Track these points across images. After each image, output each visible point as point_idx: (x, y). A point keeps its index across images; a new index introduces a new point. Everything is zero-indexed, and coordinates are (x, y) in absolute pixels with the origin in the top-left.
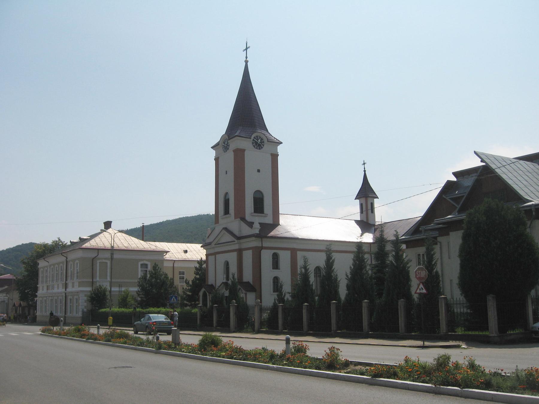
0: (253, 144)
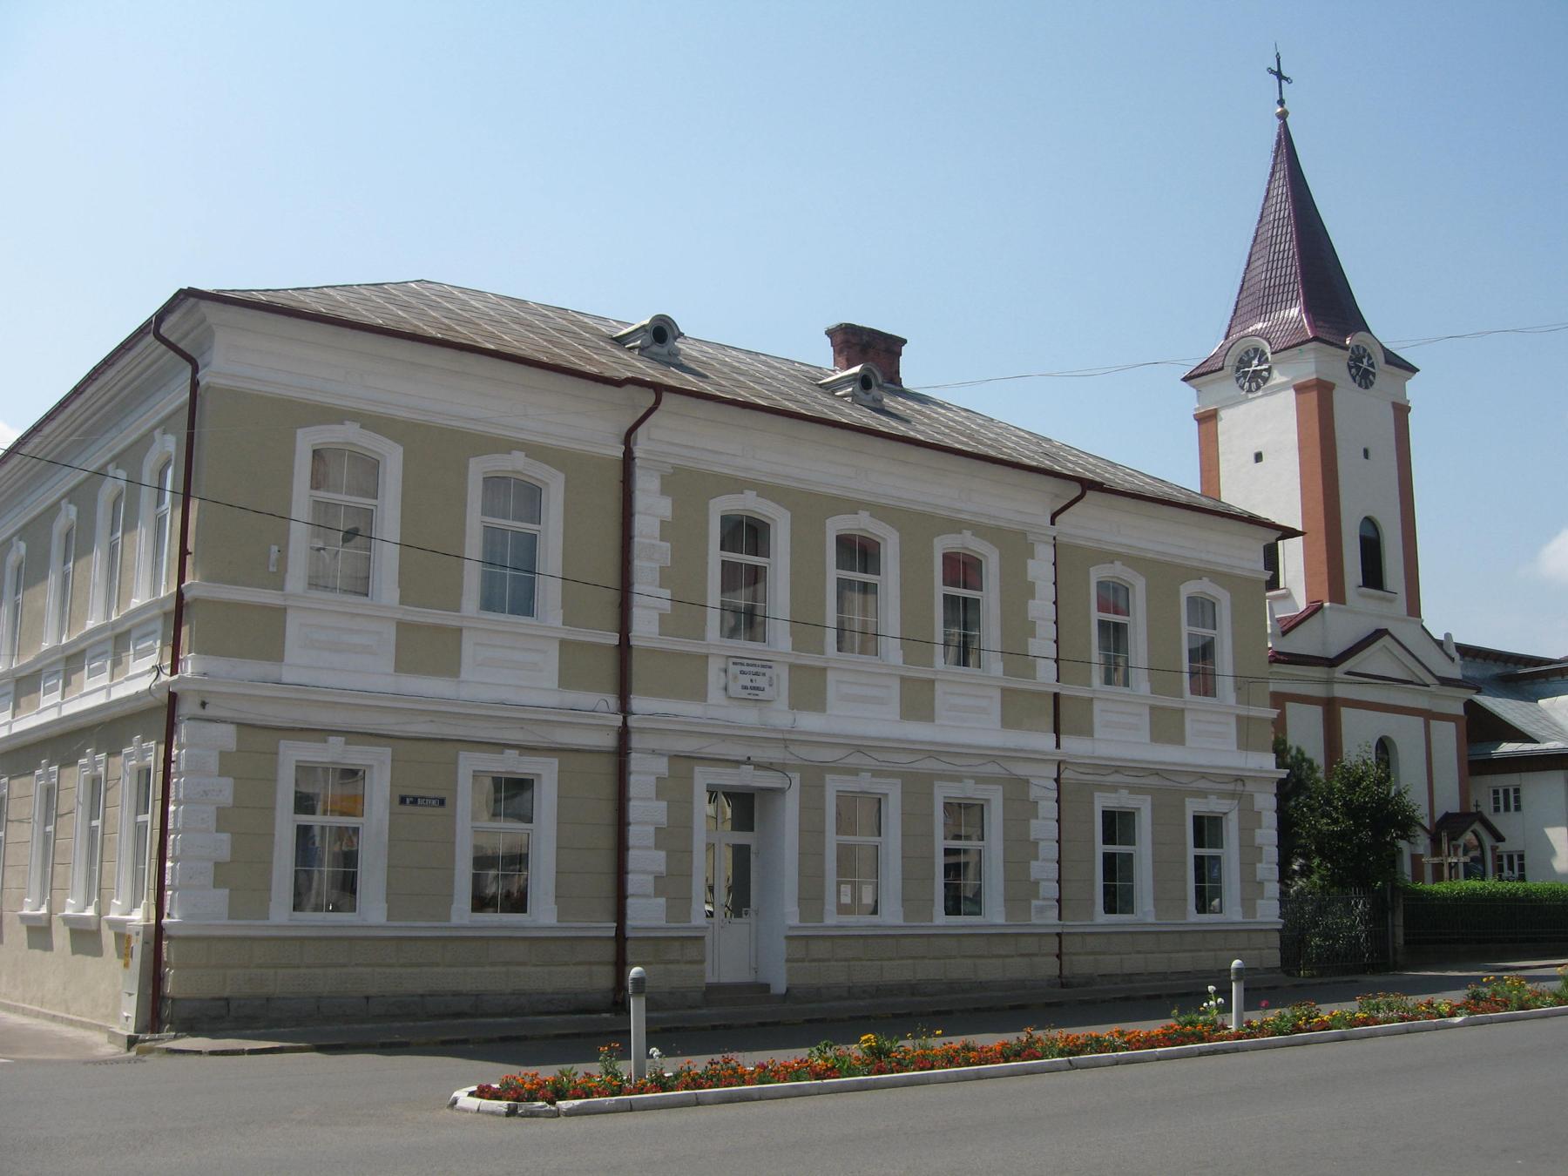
0: (1350, 371)
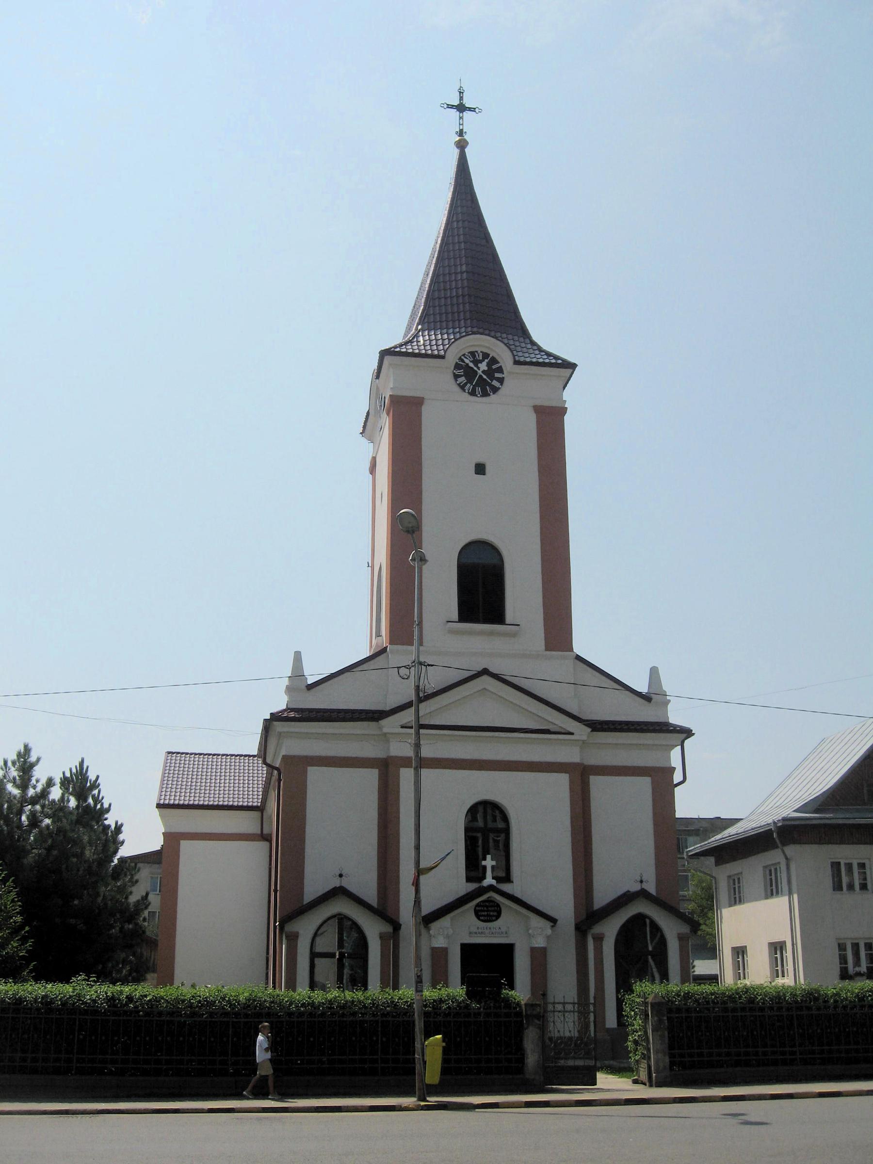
0: (456, 381)
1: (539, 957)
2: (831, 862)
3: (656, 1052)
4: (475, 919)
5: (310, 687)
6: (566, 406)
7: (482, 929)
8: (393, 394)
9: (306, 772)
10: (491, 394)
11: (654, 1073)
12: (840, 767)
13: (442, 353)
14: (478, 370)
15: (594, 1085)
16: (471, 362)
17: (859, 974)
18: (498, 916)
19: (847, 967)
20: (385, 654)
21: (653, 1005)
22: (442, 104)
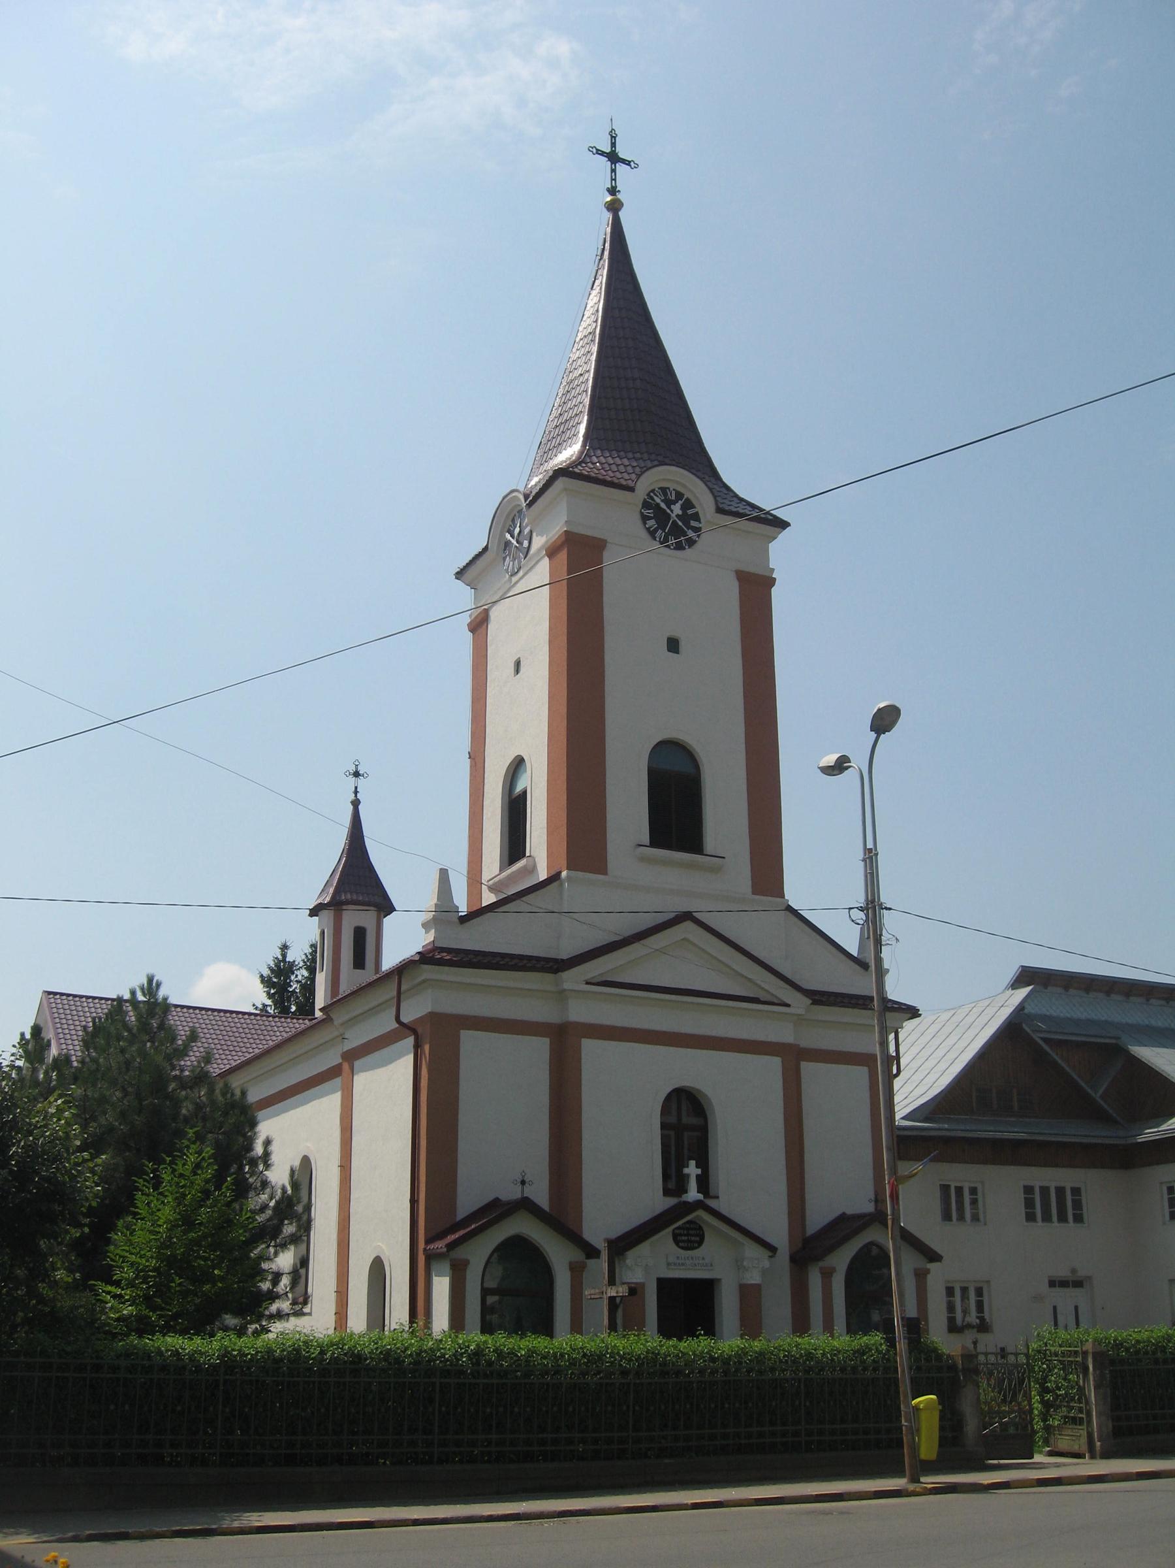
0: (645, 524)
1: (750, 1296)
2: (940, 1185)
3: (1099, 1414)
4: (674, 1246)
5: (463, 920)
6: (773, 576)
7: (690, 1258)
8: (568, 530)
9: (458, 1037)
10: (687, 547)
11: (1099, 1441)
12: (942, 1066)
13: (630, 483)
14: (671, 513)
15: (1030, 1459)
16: (662, 501)
17: (970, 1326)
18: (700, 1243)
19: (955, 1317)
20: (555, 884)
21: (1095, 1355)
22: (590, 147)
